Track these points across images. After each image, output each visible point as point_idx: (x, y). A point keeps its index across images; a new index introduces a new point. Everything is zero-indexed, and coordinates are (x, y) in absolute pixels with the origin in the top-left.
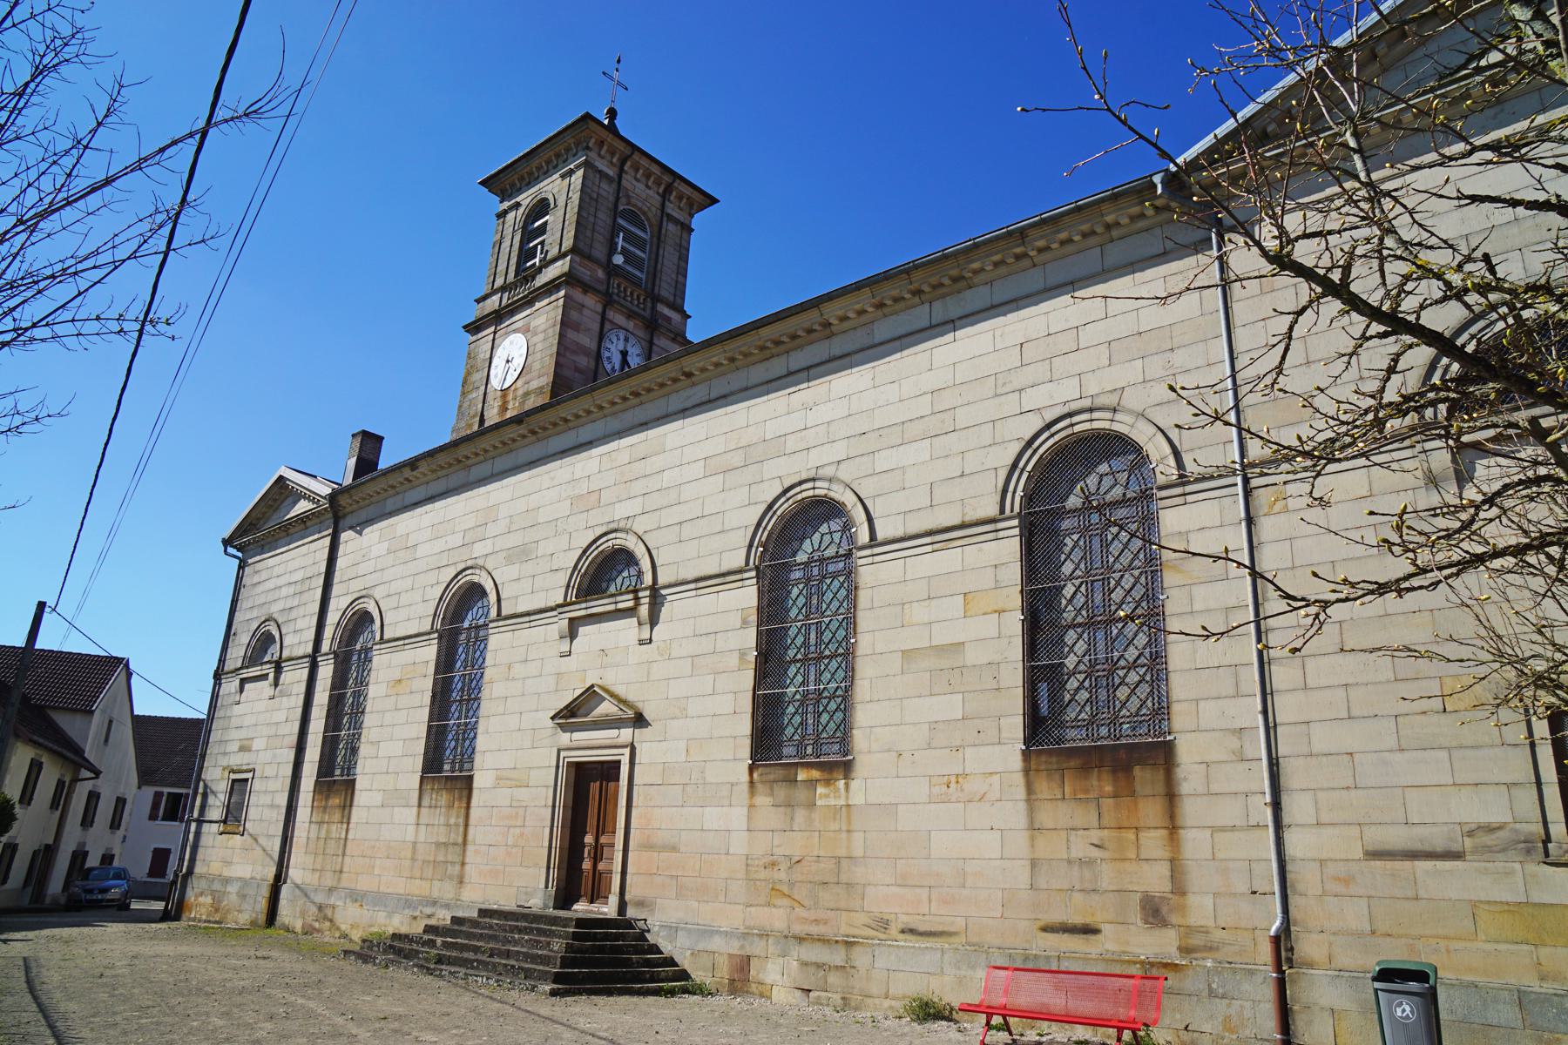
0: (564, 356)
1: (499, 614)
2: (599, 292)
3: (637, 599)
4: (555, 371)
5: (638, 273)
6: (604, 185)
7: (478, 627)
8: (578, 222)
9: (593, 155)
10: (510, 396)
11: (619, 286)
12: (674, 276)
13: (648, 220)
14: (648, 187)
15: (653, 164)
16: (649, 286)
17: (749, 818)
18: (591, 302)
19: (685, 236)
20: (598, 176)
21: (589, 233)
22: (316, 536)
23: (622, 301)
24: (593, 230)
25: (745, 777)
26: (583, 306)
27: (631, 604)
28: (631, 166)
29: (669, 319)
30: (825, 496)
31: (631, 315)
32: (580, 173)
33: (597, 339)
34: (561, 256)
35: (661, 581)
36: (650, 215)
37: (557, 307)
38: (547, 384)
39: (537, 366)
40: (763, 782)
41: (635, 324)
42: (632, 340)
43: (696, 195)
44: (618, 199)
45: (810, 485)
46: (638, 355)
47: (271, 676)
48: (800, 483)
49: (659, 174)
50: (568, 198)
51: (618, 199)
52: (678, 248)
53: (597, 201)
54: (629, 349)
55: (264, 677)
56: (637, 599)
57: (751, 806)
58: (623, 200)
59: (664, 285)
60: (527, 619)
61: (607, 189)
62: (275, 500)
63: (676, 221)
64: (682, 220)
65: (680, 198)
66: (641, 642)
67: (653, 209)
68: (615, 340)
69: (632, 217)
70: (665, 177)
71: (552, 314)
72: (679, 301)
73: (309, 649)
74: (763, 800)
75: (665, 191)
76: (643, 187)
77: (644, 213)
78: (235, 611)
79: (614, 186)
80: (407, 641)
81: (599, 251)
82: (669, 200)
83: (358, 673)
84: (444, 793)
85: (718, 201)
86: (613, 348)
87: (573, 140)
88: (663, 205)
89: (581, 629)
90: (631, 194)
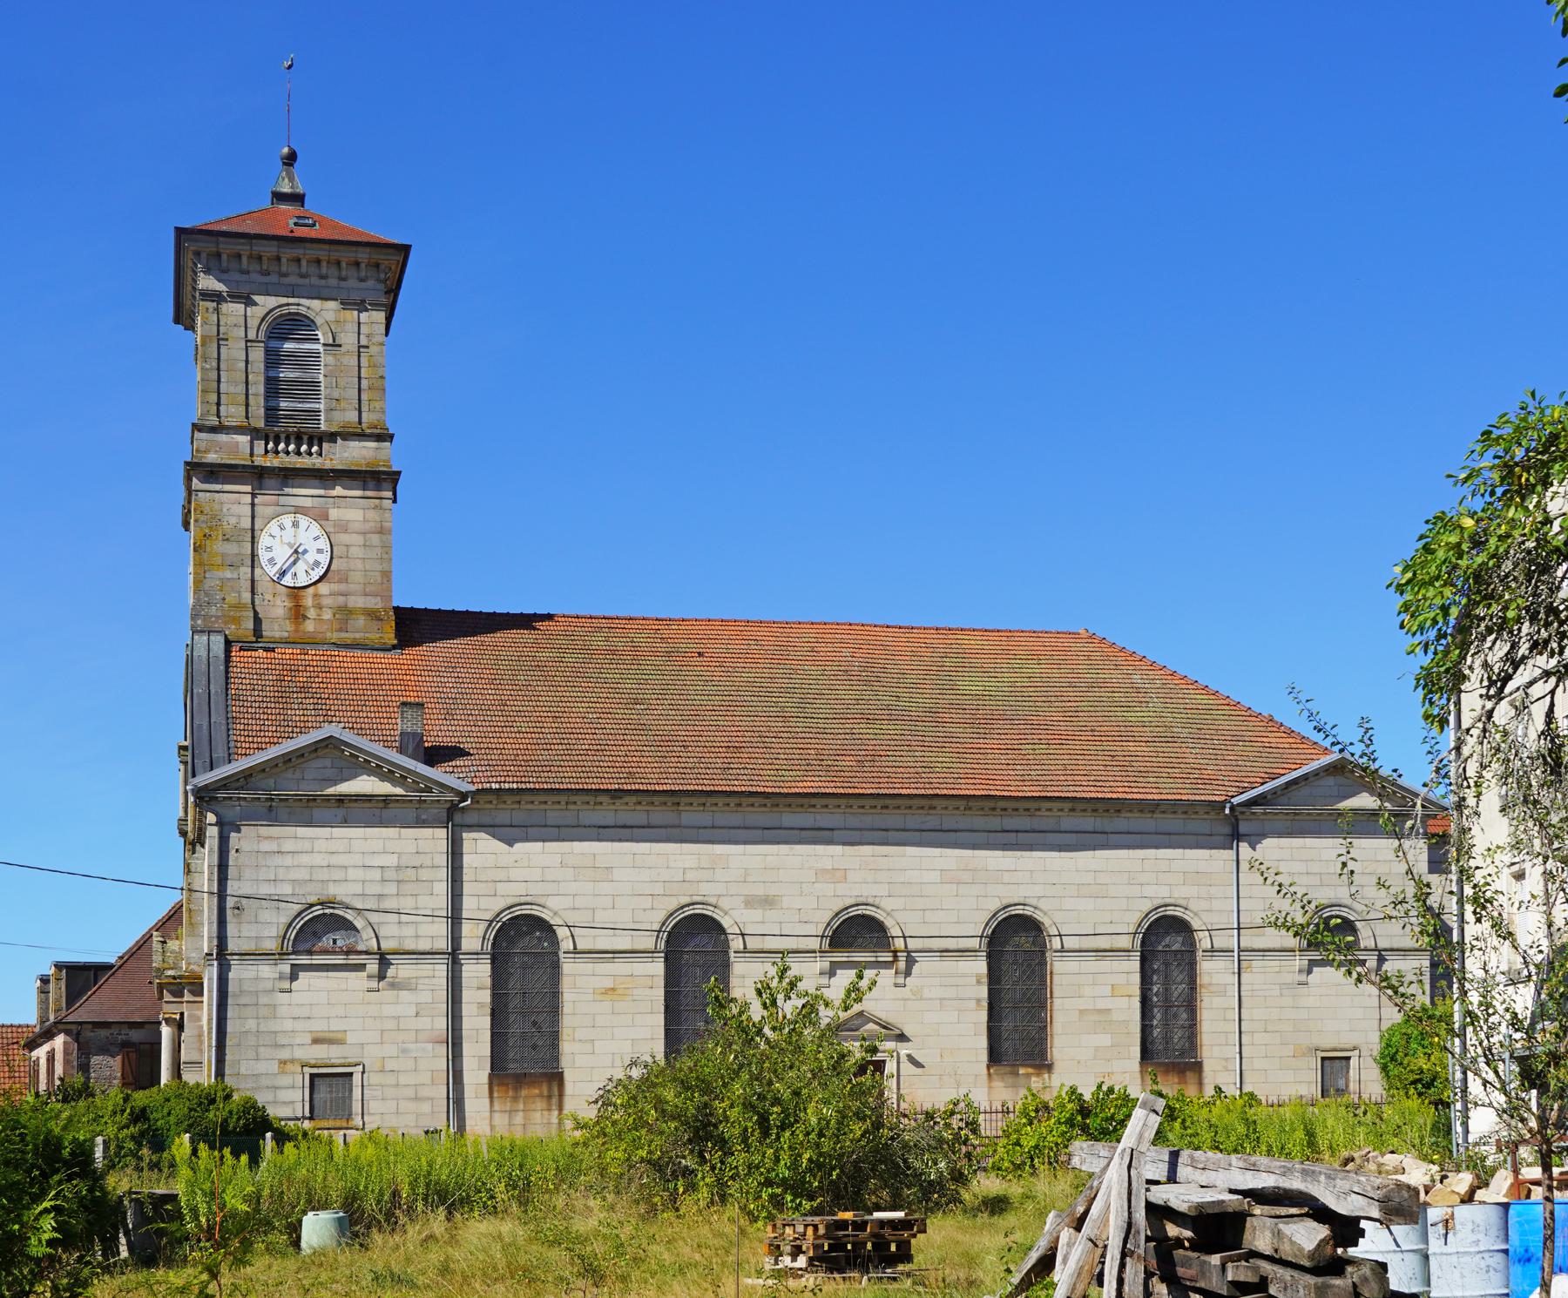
3: (895, 956)
17: (989, 1094)
25: (985, 1071)
27: (891, 959)
40: (997, 1074)
57: (990, 1087)
74: (998, 1084)
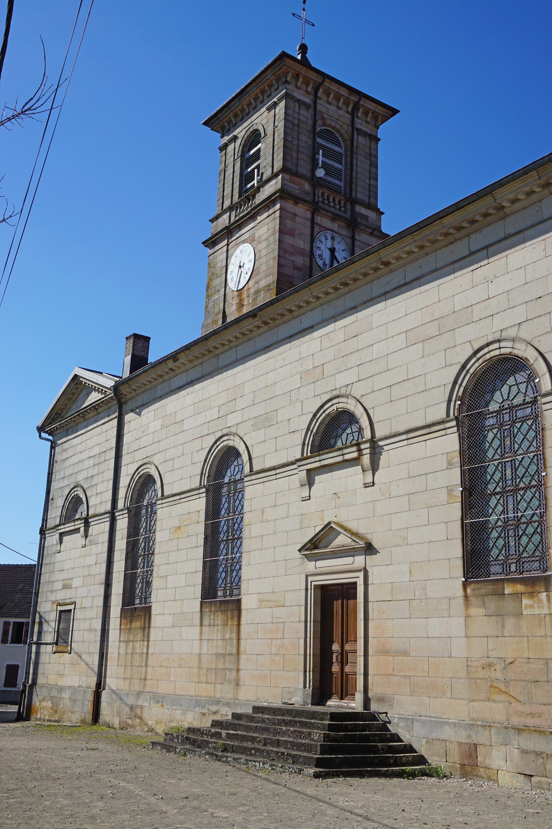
0: (284, 258)
1: (251, 470)
2: (307, 202)
3: (360, 450)
4: (278, 271)
5: (337, 182)
6: (303, 112)
7: (235, 482)
8: (285, 146)
9: (291, 87)
10: (245, 295)
11: (323, 195)
12: (367, 181)
13: (342, 136)
14: (338, 108)
15: (342, 88)
16: (348, 191)
17: (466, 626)
18: (302, 211)
19: (373, 145)
20: (297, 105)
21: (294, 154)
22: (106, 419)
23: (327, 207)
24: (298, 151)
25: (460, 592)
26: (296, 215)
27: (355, 455)
28: (323, 92)
29: (366, 218)
30: (510, 353)
31: (335, 218)
32: (282, 104)
33: (309, 241)
34: (274, 176)
35: (378, 434)
36: (343, 132)
37: (275, 218)
38: (273, 282)
39: (263, 268)
40: (475, 596)
41: (339, 225)
43: (380, 110)
44: (315, 122)
45: (496, 346)
46: (343, 250)
47: (82, 530)
48: (488, 345)
49: (347, 95)
50: (275, 127)
51: (315, 122)
52: (368, 157)
53: (298, 126)
54: (336, 246)
55: (77, 531)
56: (360, 450)
57: (467, 617)
58: (320, 122)
59: (359, 189)
60: (273, 472)
61: (306, 115)
62: (73, 394)
63: (365, 134)
64: (369, 132)
65: (366, 113)
66: (366, 486)
67: (345, 127)
68: (323, 240)
69: (329, 135)
70: (352, 98)
71: (271, 225)
72: (372, 201)
73: (109, 507)
74: (476, 611)
75: (353, 110)
76: (334, 109)
77: (338, 131)
78: (51, 482)
79: (311, 111)
80: (182, 496)
81: (304, 168)
82: (357, 117)
83: (147, 523)
84: (220, 613)
85: (398, 111)
86: (322, 247)
87: (273, 77)
88: (353, 122)
89: (316, 478)
90: (325, 116)
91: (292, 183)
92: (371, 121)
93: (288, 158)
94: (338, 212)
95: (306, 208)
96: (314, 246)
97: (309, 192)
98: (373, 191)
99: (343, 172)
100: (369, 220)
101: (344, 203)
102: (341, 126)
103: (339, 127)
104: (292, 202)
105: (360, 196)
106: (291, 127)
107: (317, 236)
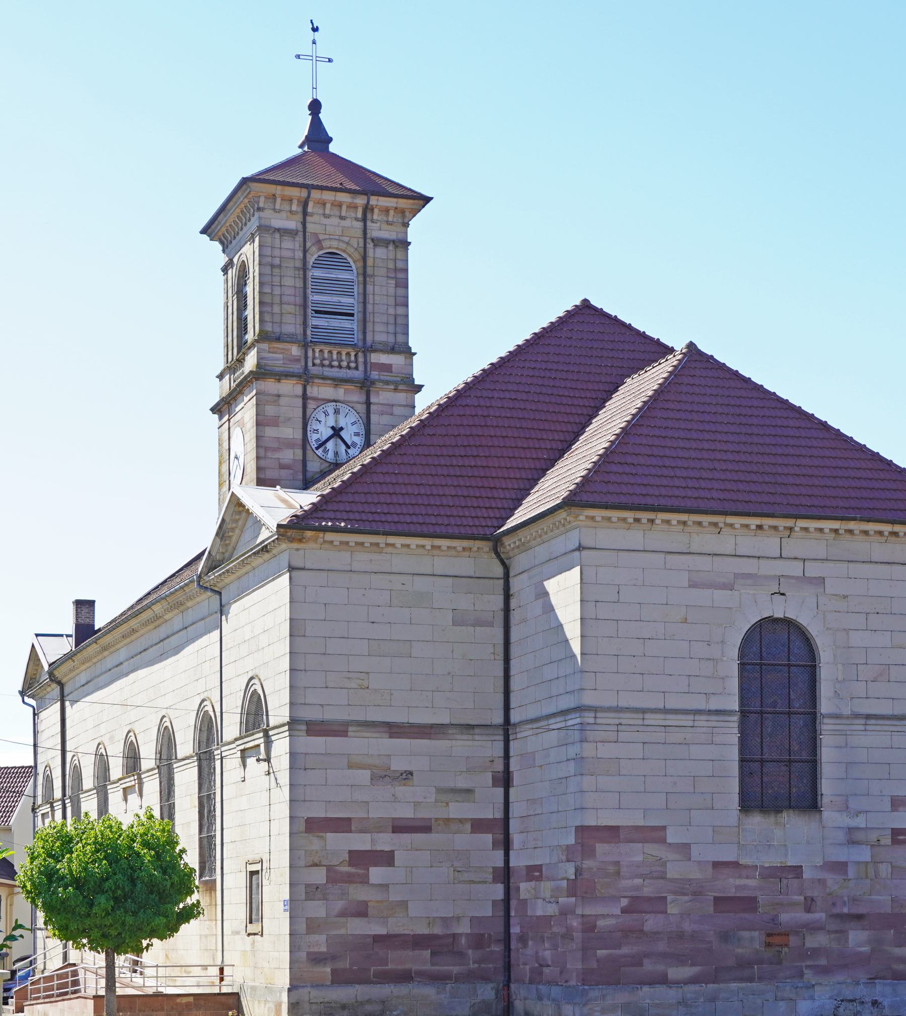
6: (288, 244)
9: (267, 214)
12: (391, 311)
13: (350, 256)
16: (361, 337)
18: (290, 387)
19: (400, 255)
20: (277, 235)
26: (279, 396)
29: (387, 368)
31: (338, 382)
36: (351, 250)
42: (344, 409)
44: (305, 251)
46: (353, 424)
51: (305, 251)
59: (378, 328)
63: (386, 243)
64: (392, 236)
68: (322, 417)
72: (400, 338)
76: (335, 221)
79: (300, 238)
82: (372, 221)
90: (321, 237)
91: (272, 353)
92: (395, 220)
93: (267, 317)
94: (344, 373)
95: (295, 382)
96: (309, 429)
97: (298, 358)
98: (401, 324)
99: (356, 308)
100: (393, 370)
101: (356, 355)
102: (348, 243)
103: (343, 246)
104: (273, 380)
105: (381, 337)
106: (269, 272)
107: (313, 415)
